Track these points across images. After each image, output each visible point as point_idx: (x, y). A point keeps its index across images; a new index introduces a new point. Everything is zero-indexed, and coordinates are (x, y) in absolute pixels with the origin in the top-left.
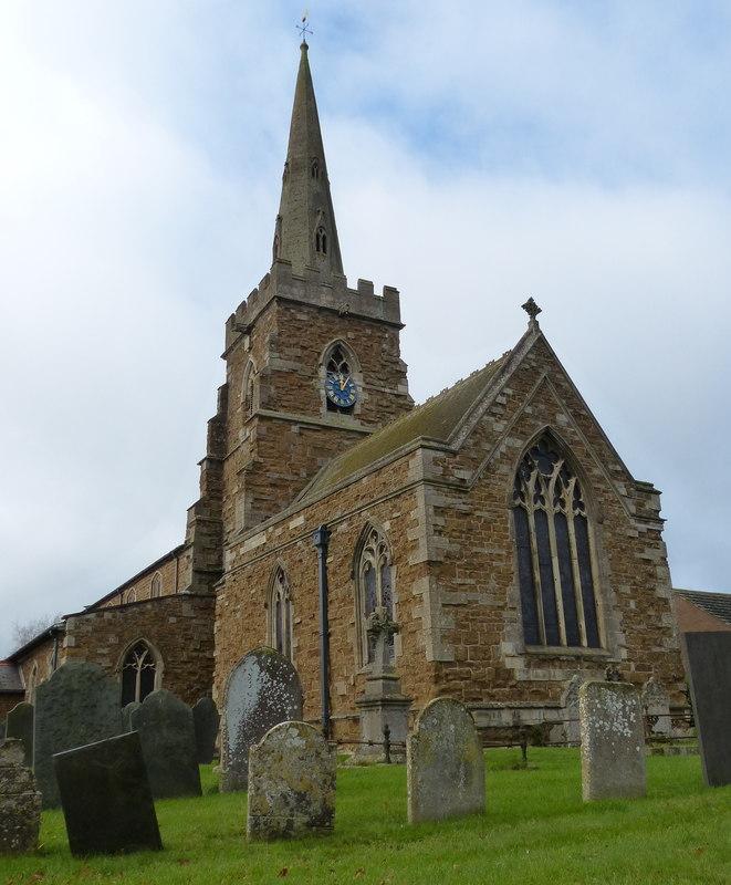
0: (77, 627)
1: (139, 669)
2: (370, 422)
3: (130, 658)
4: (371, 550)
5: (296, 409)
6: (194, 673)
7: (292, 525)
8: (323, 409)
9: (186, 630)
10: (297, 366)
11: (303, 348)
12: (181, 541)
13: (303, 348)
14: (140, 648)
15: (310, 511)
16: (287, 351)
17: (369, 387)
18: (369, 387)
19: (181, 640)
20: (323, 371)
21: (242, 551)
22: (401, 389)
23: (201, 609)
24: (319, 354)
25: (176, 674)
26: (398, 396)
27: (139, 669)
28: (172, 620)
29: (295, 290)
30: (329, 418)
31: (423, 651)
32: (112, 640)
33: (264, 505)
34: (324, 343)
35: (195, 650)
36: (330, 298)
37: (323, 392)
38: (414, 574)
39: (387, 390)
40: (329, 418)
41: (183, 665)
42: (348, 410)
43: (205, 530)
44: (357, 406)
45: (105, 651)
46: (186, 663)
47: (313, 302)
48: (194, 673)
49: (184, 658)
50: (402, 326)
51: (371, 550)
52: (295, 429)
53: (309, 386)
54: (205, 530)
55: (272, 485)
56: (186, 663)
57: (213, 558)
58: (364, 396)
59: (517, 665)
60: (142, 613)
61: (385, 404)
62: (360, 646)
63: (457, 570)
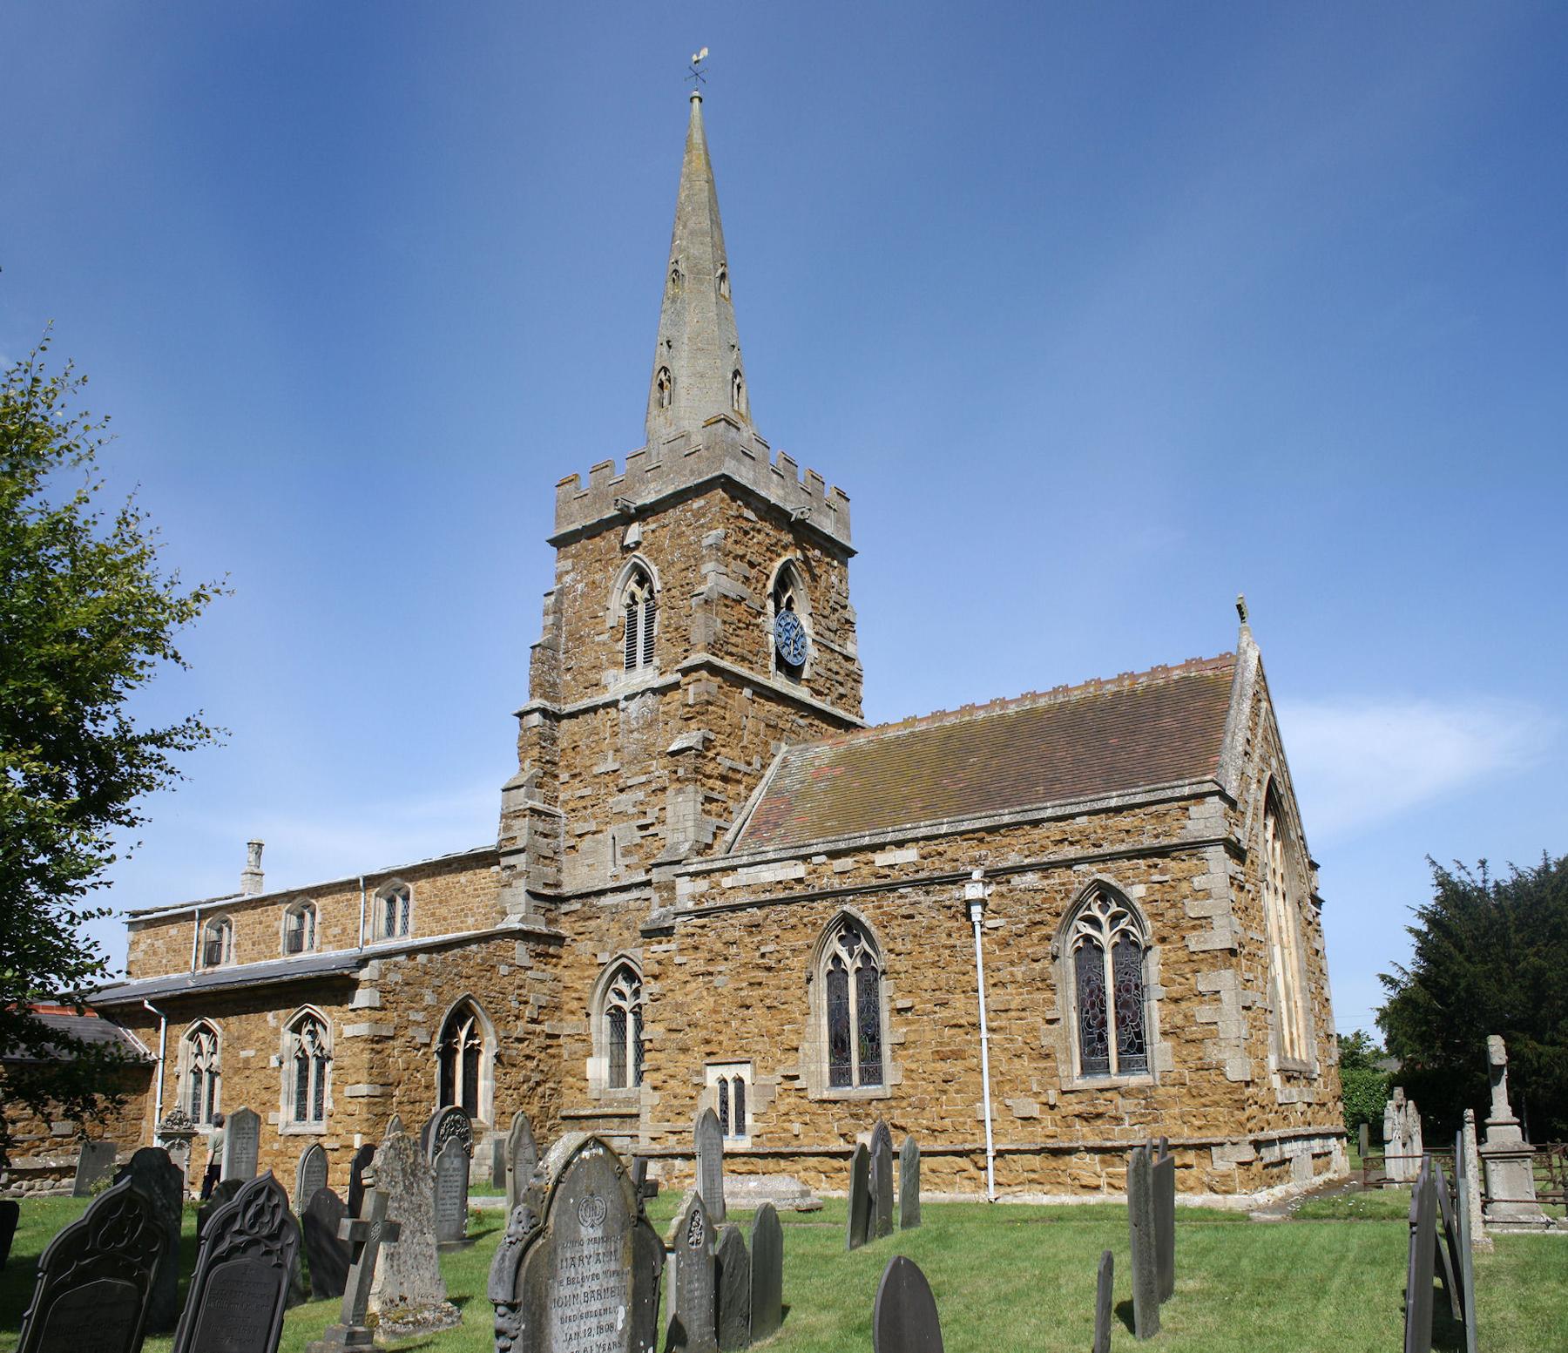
0: (383, 975)
1: (461, 1048)
2: (819, 693)
3: (449, 1033)
4: (1094, 922)
5: (743, 659)
6: (528, 1057)
7: (881, 859)
8: (772, 666)
9: (520, 987)
10: (746, 591)
11: (752, 565)
12: (487, 839)
13: (752, 565)
14: (462, 1013)
15: (932, 847)
16: (737, 566)
17: (818, 638)
18: (818, 638)
19: (514, 1004)
20: (770, 605)
21: (727, 882)
22: (850, 649)
23: (538, 955)
24: (768, 577)
25: (510, 1056)
26: (847, 658)
27: (461, 1048)
28: (503, 970)
29: (743, 470)
30: (779, 683)
31: (1219, 1068)
32: (429, 998)
33: (713, 807)
34: (771, 560)
35: (533, 1021)
36: (781, 492)
37: (771, 638)
38: (1198, 961)
39: (837, 648)
40: (779, 683)
41: (516, 1045)
42: (793, 672)
43: (541, 826)
44: (807, 666)
45: (420, 1017)
46: (520, 1040)
47: (763, 494)
48: (528, 1057)
49: (519, 1033)
50: (851, 553)
51: (1094, 922)
52: (747, 692)
53: (757, 626)
54: (541, 826)
55: (725, 779)
56: (520, 1040)
57: (550, 870)
58: (812, 651)
59: (1276, 1081)
60: (465, 958)
61: (835, 668)
62: (1068, 1050)
63: (1244, 961)
